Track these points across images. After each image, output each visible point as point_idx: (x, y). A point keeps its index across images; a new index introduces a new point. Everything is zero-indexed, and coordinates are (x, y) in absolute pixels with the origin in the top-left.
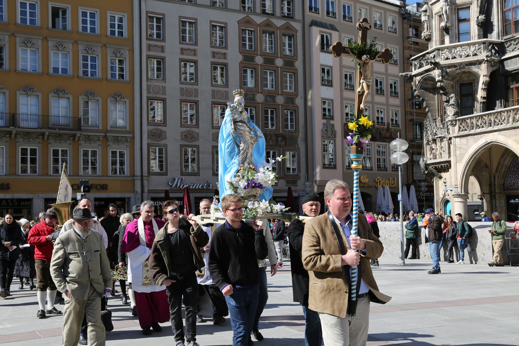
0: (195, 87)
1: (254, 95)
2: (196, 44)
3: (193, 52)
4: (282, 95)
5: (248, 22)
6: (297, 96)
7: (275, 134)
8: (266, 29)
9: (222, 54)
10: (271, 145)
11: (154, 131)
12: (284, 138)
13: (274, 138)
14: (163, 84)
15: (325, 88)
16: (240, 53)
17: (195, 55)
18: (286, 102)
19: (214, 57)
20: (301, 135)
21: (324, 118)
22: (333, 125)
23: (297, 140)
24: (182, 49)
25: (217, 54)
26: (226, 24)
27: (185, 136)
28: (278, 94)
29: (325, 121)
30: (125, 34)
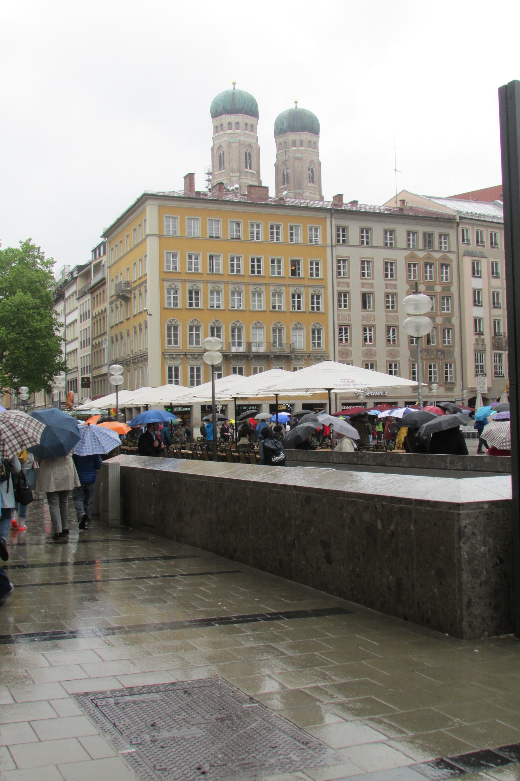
0: (373, 313)
2: (373, 279)
4: (441, 316)
5: (413, 256)
6: (453, 316)
7: (436, 349)
8: (427, 261)
10: (433, 359)
11: (343, 351)
12: (443, 352)
13: (435, 352)
16: (407, 283)
17: (372, 287)
19: (387, 288)
20: (457, 349)
21: (476, 334)
22: (483, 339)
23: (453, 353)
24: (363, 284)
25: (389, 285)
26: (395, 260)
27: (366, 353)
28: (438, 316)
29: (477, 337)
30: (321, 276)
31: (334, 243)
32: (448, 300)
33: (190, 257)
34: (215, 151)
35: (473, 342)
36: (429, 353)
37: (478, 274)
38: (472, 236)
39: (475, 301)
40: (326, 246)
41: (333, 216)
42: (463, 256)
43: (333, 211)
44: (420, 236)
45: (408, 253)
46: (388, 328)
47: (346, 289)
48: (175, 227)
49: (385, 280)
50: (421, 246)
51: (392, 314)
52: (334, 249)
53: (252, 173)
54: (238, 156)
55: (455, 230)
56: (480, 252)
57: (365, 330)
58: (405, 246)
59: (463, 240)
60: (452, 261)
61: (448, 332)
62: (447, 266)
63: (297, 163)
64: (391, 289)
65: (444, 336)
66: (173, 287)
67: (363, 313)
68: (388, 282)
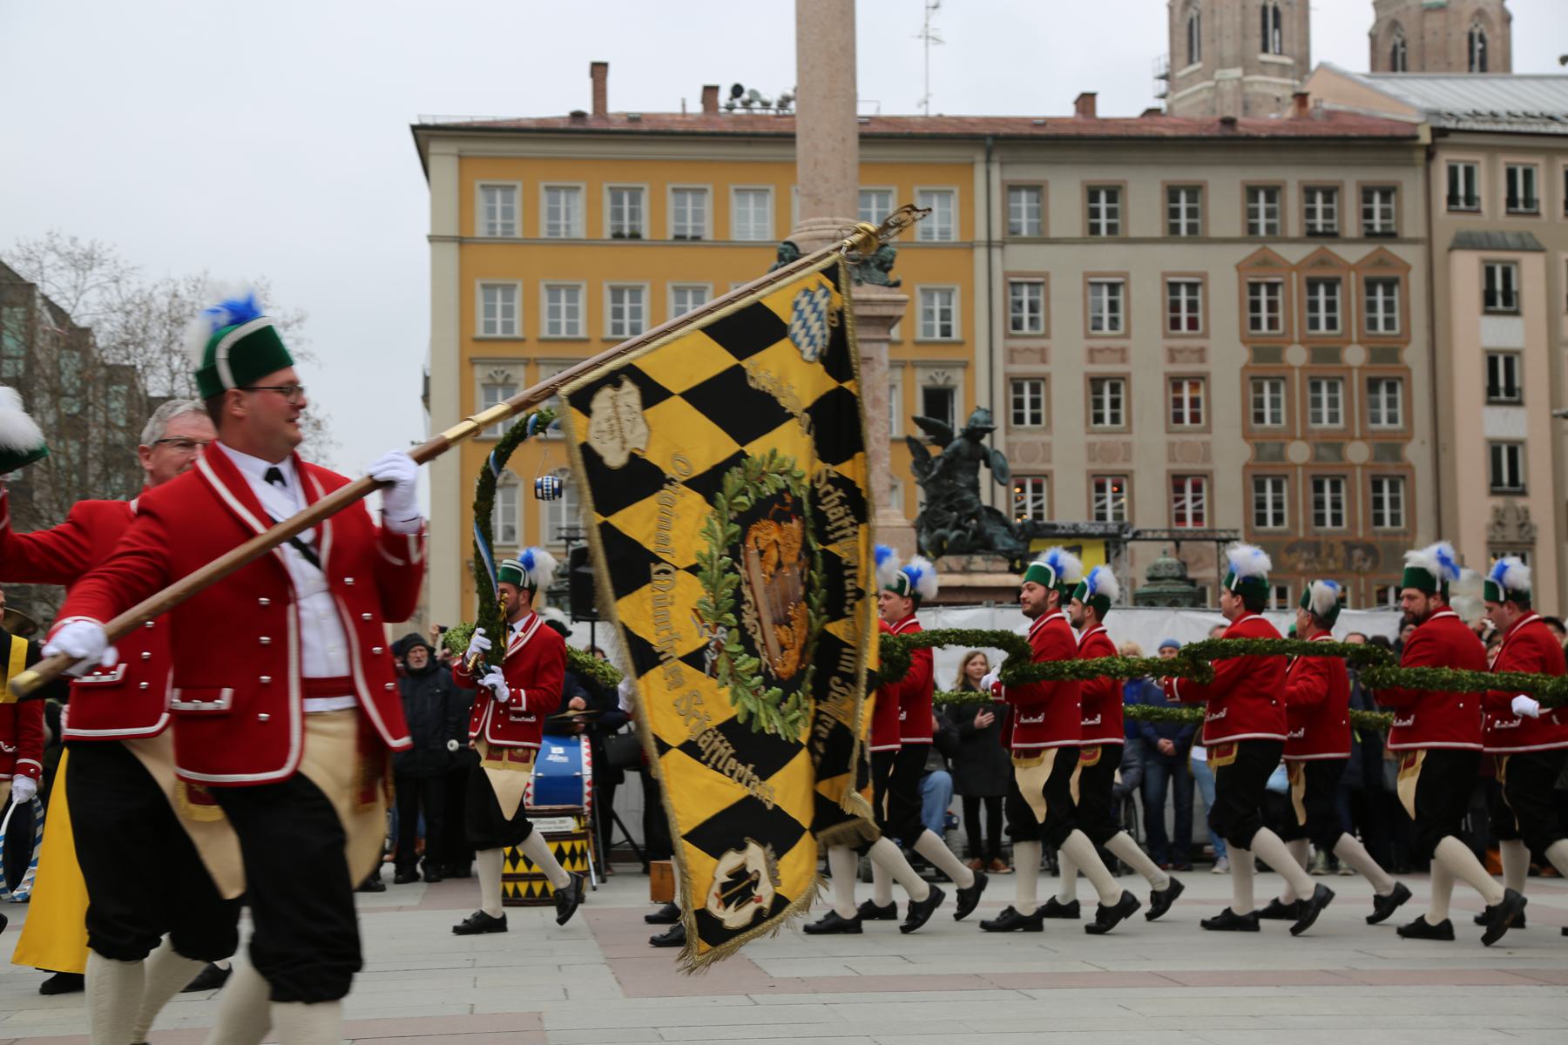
1: (1282, 445)
2: (1127, 336)
3: (1118, 356)
4: (1363, 438)
5: (1265, 262)
7: (1345, 543)
9: (1193, 351)
12: (1370, 550)
13: (1340, 551)
14: (1045, 438)
15: (1498, 411)
16: (1244, 342)
17: (1124, 360)
18: (1376, 457)
19: (1172, 360)
21: (1494, 493)
24: (1091, 351)
25: (1181, 351)
26: (1204, 275)
28: (1353, 438)
29: (1499, 502)
30: (956, 335)
31: (997, 235)
32: (1391, 388)
33: (617, 293)
34: (1177, 10)
35: (1488, 518)
36: (1318, 553)
37: (1508, 299)
38: (1490, 186)
39: (1492, 390)
40: (971, 246)
41: (995, 157)
42: (1451, 249)
43: (989, 142)
44: (1293, 202)
45: (1248, 250)
46: (1177, 482)
47: (1036, 369)
48: (508, 213)
49: (1166, 336)
50: (1294, 227)
51: (1192, 438)
52: (996, 253)
53: (1283, 66)
54: (1238, 19)
55: (1420, 171)
56: (1520, 236)
57: (1101, 488)
58: (1236, 229)
59: (1453, 198)
60: (1408, 268)
61: (1394, 488)
62: (1389, 285)
63: (1434, 22)
64: (1188, 361)
65: (1378, 503)
66: (500, 379)
67: (1093, 438)
68: (1177, 343)
